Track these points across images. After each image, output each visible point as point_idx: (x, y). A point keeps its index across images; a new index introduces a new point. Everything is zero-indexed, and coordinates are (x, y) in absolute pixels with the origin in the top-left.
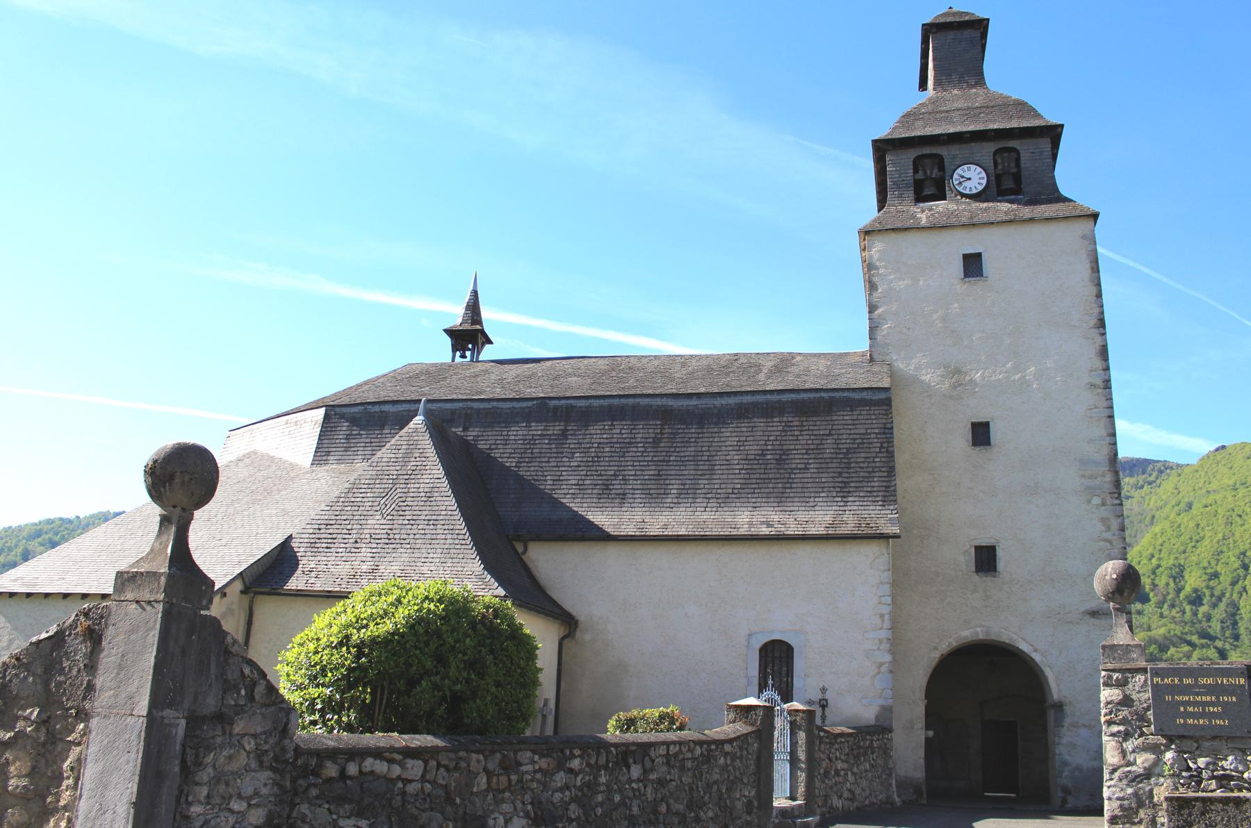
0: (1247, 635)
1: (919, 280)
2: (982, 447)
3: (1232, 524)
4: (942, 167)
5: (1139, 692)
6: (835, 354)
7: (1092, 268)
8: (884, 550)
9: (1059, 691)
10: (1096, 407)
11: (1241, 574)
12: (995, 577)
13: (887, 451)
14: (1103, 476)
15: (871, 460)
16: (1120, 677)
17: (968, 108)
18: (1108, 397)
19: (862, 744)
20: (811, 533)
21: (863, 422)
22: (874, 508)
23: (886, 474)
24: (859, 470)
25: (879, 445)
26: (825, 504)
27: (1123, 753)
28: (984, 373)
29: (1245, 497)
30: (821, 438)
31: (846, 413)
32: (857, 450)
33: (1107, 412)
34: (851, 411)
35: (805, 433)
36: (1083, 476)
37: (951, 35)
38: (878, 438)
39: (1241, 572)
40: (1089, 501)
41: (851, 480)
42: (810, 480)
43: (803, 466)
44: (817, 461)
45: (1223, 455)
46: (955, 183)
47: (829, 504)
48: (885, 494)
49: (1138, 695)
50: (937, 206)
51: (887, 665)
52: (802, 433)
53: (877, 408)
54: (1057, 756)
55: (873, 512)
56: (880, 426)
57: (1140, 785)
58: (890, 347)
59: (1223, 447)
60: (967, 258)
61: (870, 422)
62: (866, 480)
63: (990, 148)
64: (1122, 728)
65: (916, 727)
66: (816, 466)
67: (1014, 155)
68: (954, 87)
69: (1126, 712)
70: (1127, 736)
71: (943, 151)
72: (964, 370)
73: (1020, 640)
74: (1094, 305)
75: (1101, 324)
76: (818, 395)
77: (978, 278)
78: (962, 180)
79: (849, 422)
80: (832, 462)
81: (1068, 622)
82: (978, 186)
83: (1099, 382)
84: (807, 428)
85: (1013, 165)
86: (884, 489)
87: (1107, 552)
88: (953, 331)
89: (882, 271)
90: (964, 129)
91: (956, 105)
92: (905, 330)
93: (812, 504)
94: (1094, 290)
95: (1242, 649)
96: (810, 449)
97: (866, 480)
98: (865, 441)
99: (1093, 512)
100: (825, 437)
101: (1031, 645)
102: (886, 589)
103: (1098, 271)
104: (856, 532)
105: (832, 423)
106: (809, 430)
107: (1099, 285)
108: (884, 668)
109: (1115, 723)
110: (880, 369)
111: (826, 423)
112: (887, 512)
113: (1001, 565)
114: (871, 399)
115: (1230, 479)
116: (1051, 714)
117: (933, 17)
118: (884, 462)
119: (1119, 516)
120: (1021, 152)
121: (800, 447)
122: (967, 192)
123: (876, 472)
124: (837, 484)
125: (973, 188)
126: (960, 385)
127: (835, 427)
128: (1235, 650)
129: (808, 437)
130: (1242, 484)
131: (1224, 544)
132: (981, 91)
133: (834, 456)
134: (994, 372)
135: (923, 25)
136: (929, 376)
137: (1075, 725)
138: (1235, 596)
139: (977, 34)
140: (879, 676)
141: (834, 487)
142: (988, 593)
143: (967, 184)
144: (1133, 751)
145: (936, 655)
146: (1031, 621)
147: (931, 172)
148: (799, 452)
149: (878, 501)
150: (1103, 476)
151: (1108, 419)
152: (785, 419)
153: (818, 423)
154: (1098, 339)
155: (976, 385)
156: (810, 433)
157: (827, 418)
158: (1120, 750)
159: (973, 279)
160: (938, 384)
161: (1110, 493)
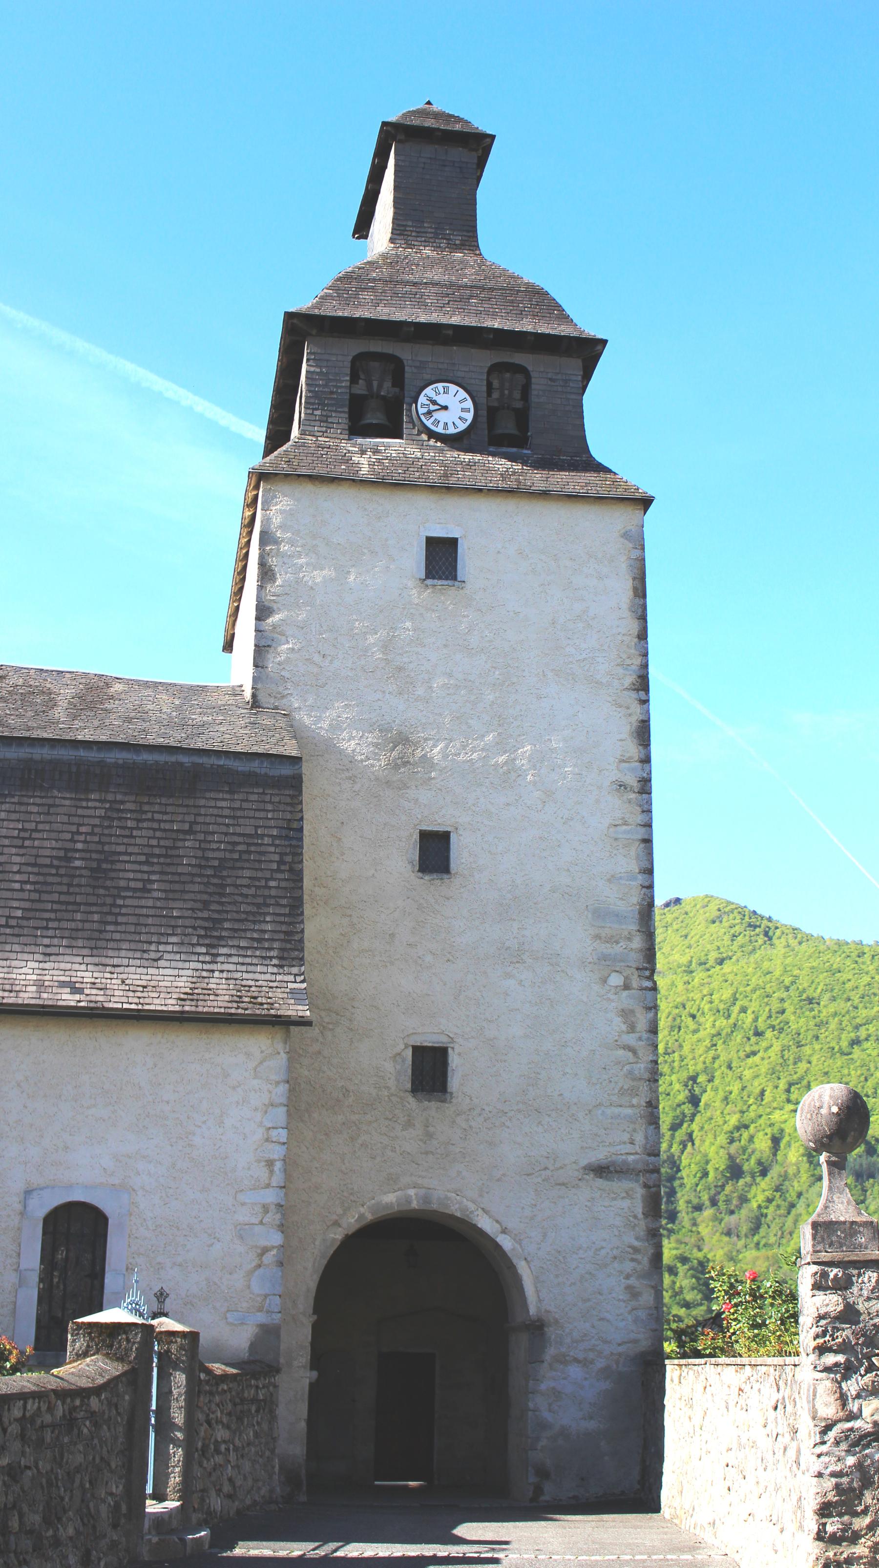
0: (688, 1213)
1: (349, 572)
2: (435, 876)
3: (680, 1028)
4: (399, 379)
5: (869, 1299)
6: (181, 686)
7: (635, 589)
8: (280, 1046)
9: (540, 1301)
10: (625, 823)
11: (686, 1111)
12: (444, 1101)
13: (291, 870)
14: (629, 939)
15: (263, 883)
16: (840, 1274)
17: (451, 285)
18: (646, 807)
19: (246, 1395)
20: (152, 1007)
21: (251, 814)
22: (264, 969)
23: (287, 911)
24: (240, 899)
25: (277, 857)
26: (177, 957)
27: (843, 1399)
28: (447, 747)
29: (702, 985)
30: (174, 835)
31: (221, 796)
32: (238, 864)
33: (641, 833)
34: (231, 792)
35: (145, 825)
36: (597, 937)
37: (428, 151)
38: (277, 846)
39: (688, 1109)
40: (604, 981)
41: (225, 916)
42: (151, 912)
43: (140, 885)
44: (165, 878)
45: (675, 915)
46: (422, 411)
47: (183, 957)
48: (284, 945)
49: (866, 1304)
50: (388, 446)
51: (274, 1252)
52: (140, 825)
53: (276, 791)
54: (530, 1413)
55: (263, 977)
56: (280, 823)
57: (867, 1451)
58: (289, 685)
59: (678, 901)
60: (432, 543)
61: (262, 814)
62: (251, 918)
63: (483, 359)
64: (841, 1358)
65: (295, 1363)
66: (163, 886)
67: (520, 378)
68: (426, 243)
69: (848, 1332)
70: (848, 1371)
71: (405, 352)
72: (413, 737)
73: (480, 1212)
74: (633, 651)
75: (643, 684)
76: (173, 759)
77: (450, 582)
78: (432, 407)
79: (226, 812)
80: (192, 882)
81: (559, 1184)
82: (459, 423)
83: (632, 780)
84: (149, 816)
85: (517, 395)
86: (282, 936)
87: (627, 1067)
88: (400, 669)
89: (285, 548)
90: (444, 320)
91: (429, 275)
92: (317, 658)
93: (153, 955)
94: (634, 627)
95: (680, 1236)
96: (153, 855)
97: (251, 918)
98: (253, 848)
99: (609, 999)
100: (181, 836)
101: (497, 1221)
102: (280, 1114)
103: (644, 596)
104: (233, 1011)
105: (194, 811)
106: (152, 820)
107: (643, 618)
108: (269, 1258)
109: (830, 1350)
110: (273, 721)
111: (184, 810)
112: (286, 978)
113: (454, 1082)
114: (266, 775)
115: (683, 954)
116: (520, 1344)
117: (400, 114)
118: (285, 888)
119: (650, 1009)
120: (533, 374)
121: (136, 850)
122: (440, 429)
123: (268, 905)
124: (199, 923)
125: (450, 425)
126: (406, 763)
127: (200, 819)
128: (669, 1237)
129: (150, 833)
130: (701, 964)
131: (666, 1062)
132: (471, 259)
133: (195, 871)
134: (464, 747)
135: (384, 124)
136: (353, 743)
137: (562, 1360)
138: (675, 1149)
139: (473, 157)
140: (261, 1270)
141: (194, 928)
142: (431, 1129)
143: (441, 416)
144: (858, 1396)
145: (337, 1235)
146: (498, 1180)
147: (380, 386)
148: (133, 858)
149: (271, 958)
150: (629, 939)
151: (642, 845)
152: (110, 797)
153: (170, 809)
154: (636, 709)
155: (433, 766)
156: (155, 825)
157: (186, 802)
158: (837, 1395)
159: (440, 582)
160: (368, 759)
161: (638, 969)
